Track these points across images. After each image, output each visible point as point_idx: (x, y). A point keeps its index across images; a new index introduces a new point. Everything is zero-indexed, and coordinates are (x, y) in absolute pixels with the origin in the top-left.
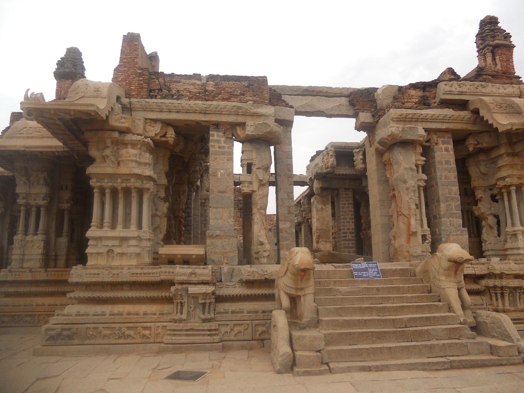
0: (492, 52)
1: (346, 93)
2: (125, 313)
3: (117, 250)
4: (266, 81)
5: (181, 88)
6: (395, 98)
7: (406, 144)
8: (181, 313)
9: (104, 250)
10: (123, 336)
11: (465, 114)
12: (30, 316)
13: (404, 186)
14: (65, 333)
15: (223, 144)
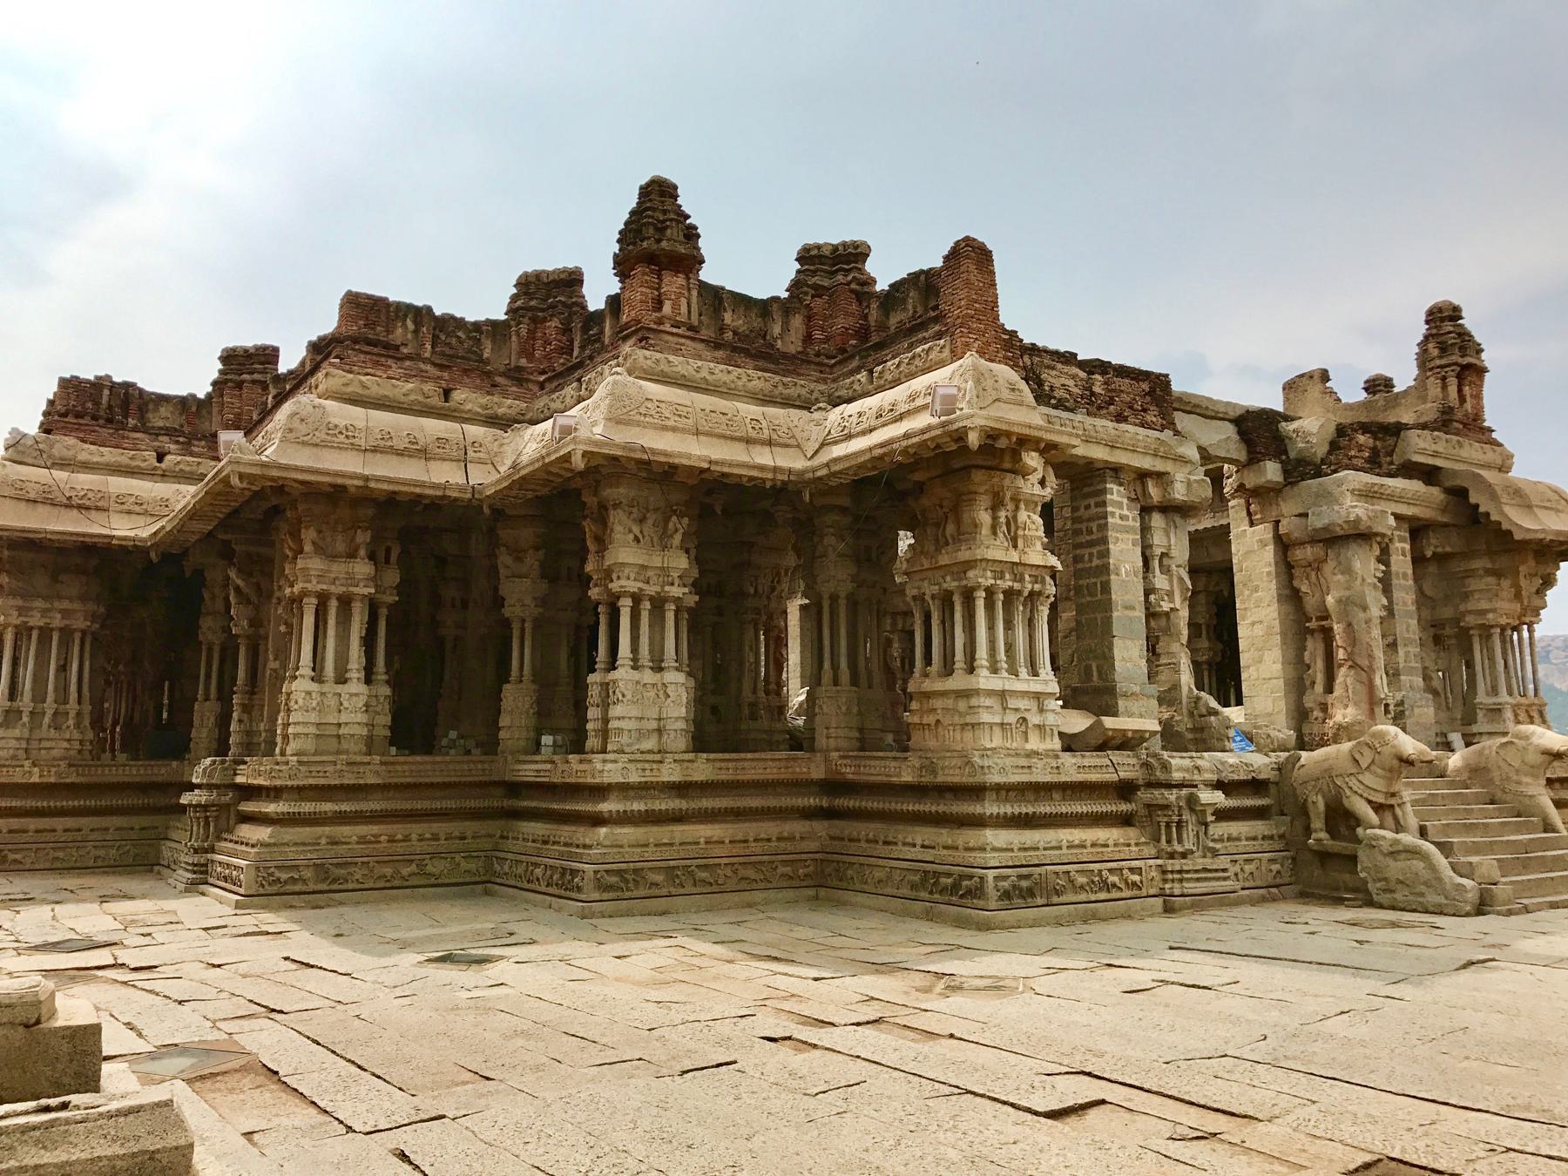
0: (1458, 376)
1: (1232, 414)
2: (1064, 843)
3: (1034, 719)
4: (1168, 383)
5: (1057, 383)
6: (1334, 446)
7: (1362, 536)
8: (1180, 841)
9: (1011, 718)
10: (1108, 887)
11: (1435, 493)
12: (706, 866)
13: (1362, 615)
14: (1024, 884)
15: (1125, 512)
